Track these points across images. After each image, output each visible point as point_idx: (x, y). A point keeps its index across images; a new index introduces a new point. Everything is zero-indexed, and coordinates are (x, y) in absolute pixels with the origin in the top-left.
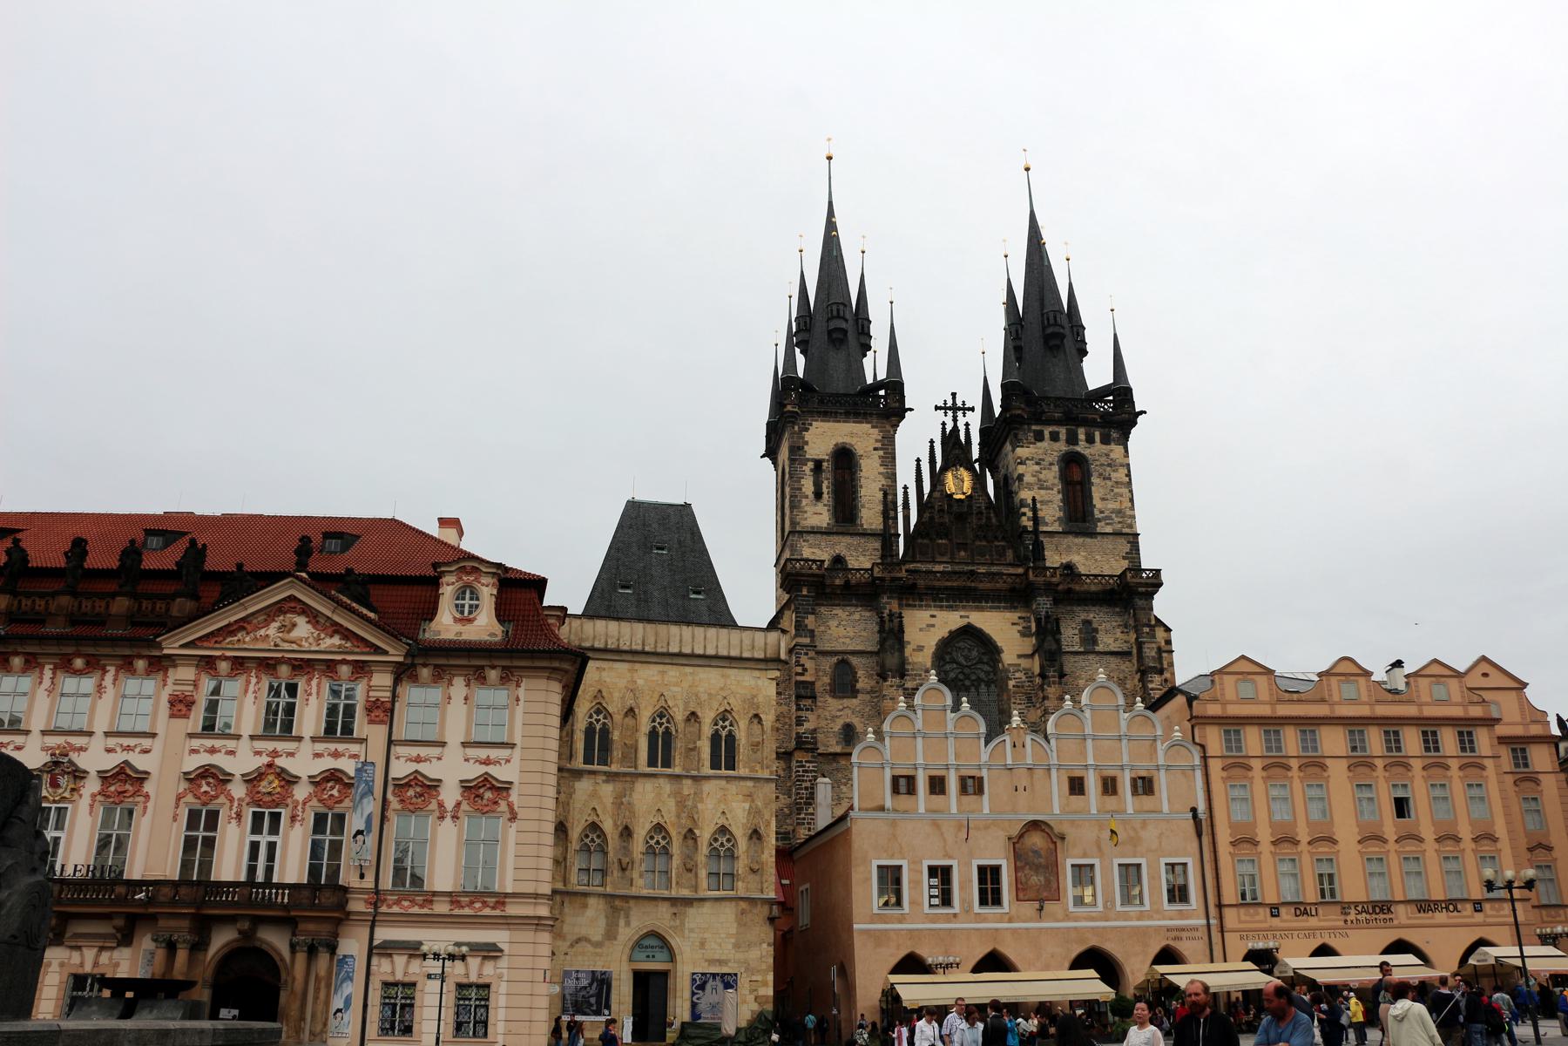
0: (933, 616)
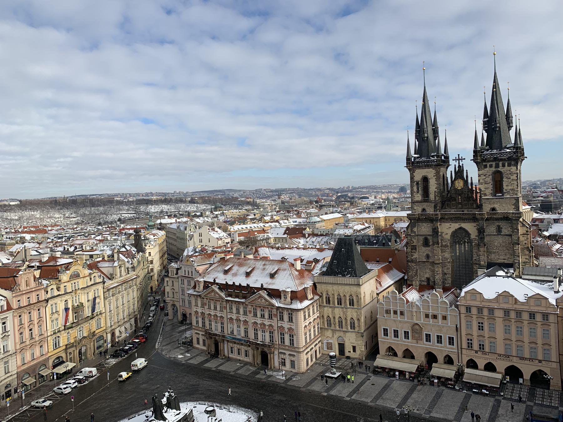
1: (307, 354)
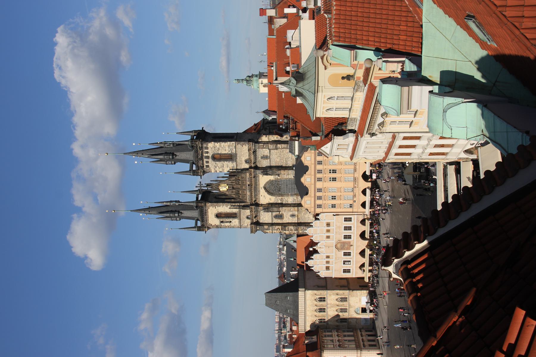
0: (262, 196)
1: (364, 346)
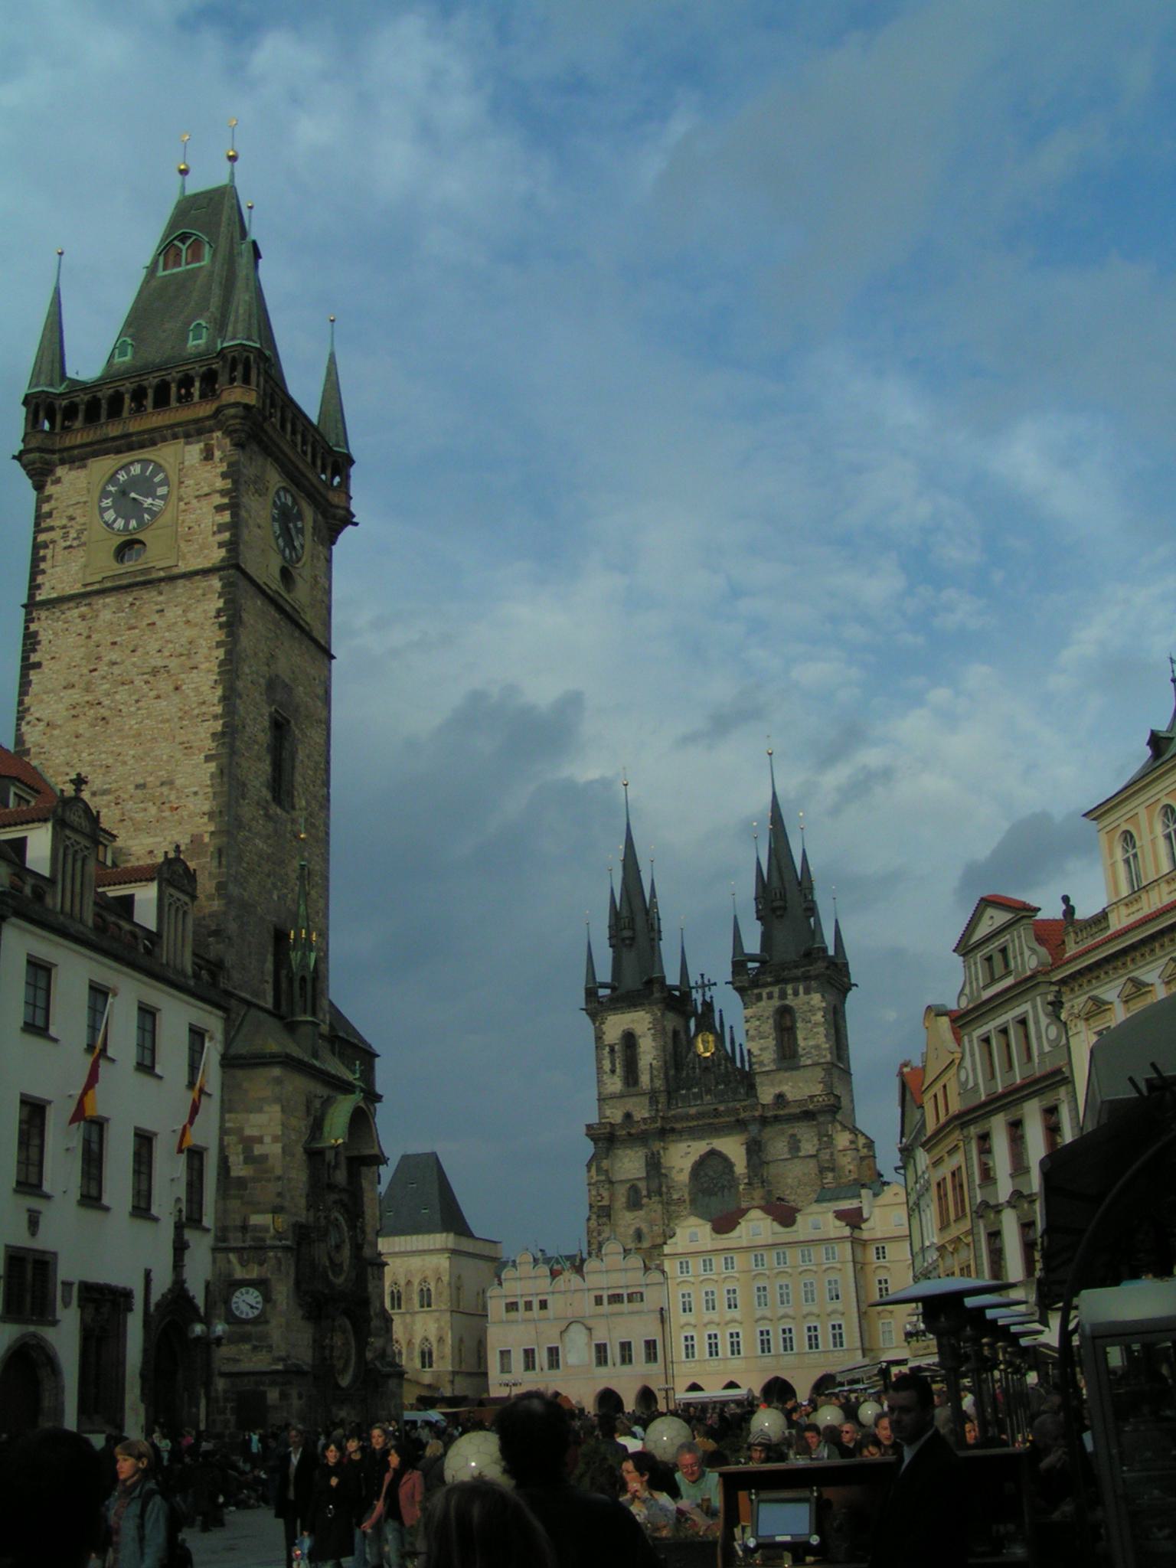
0: (689, 1146)
